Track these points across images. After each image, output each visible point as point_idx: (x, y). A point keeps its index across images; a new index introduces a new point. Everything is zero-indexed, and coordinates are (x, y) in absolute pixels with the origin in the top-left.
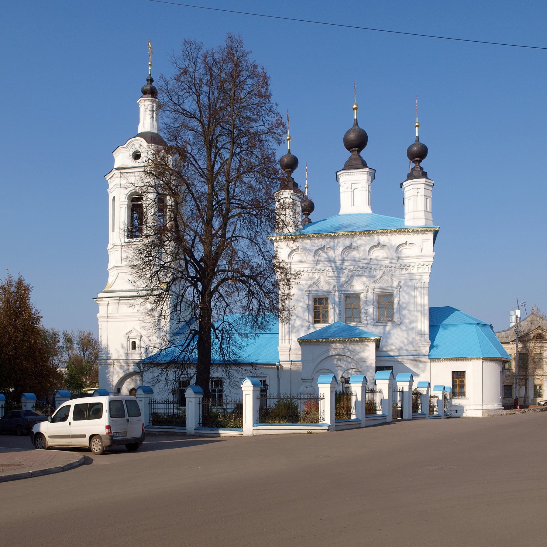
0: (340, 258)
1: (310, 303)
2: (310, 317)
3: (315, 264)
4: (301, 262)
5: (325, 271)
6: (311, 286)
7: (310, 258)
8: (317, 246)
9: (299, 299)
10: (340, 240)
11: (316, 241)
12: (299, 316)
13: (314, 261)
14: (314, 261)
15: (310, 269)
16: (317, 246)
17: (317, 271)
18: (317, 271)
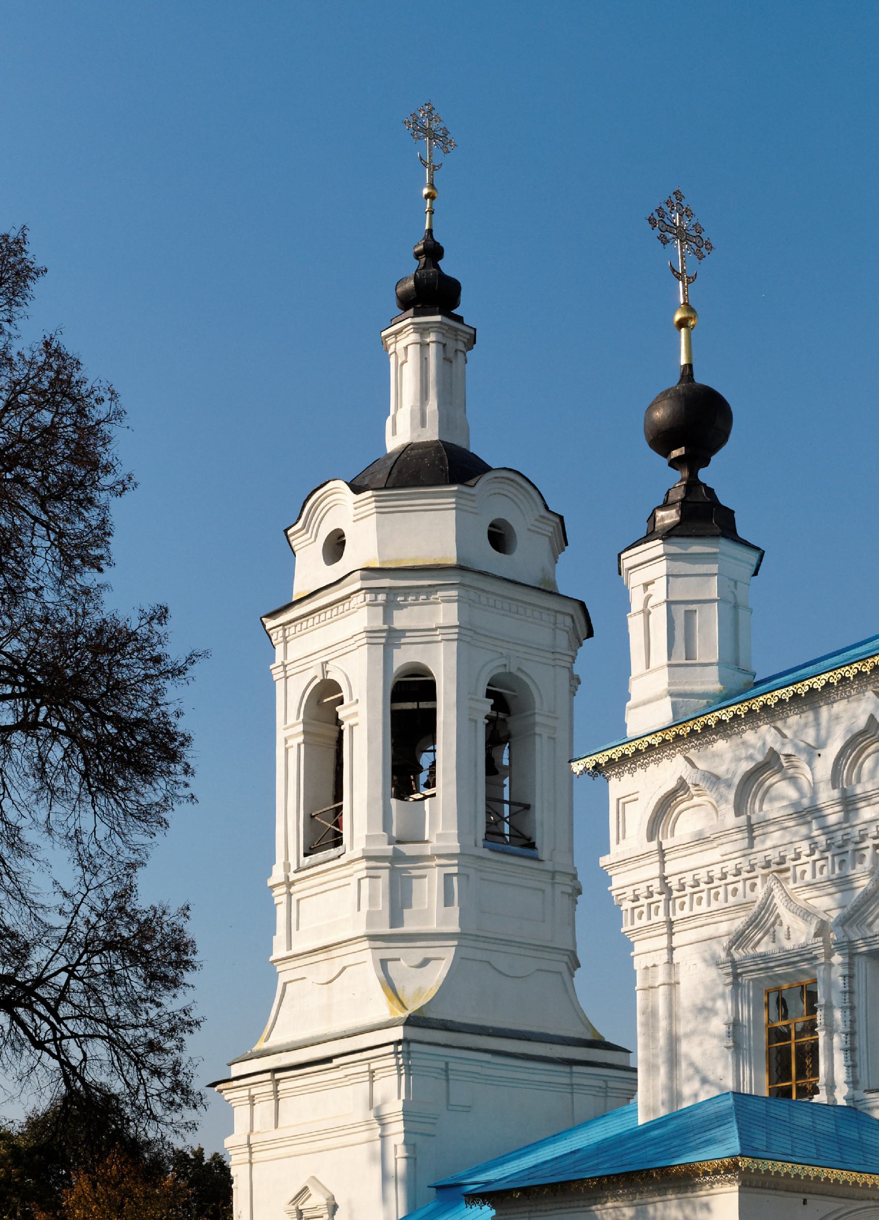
0: (836, 794)
1: (745, 1013)
2: (746, 1072)
3: (745, 843)
4: (701, 840)
5: (789, 864)
6: (739, 939)
7: (730, 819)
8: (750, 758)
9: (709, 1004)
10: (838, 707)
11: (749, 736)
12: (712, 1077)
13: (739, 829)
14: (739, 829)
15: (730, 867)
16: (750, 758)
17: (759, 871)
18: (759, 871)
